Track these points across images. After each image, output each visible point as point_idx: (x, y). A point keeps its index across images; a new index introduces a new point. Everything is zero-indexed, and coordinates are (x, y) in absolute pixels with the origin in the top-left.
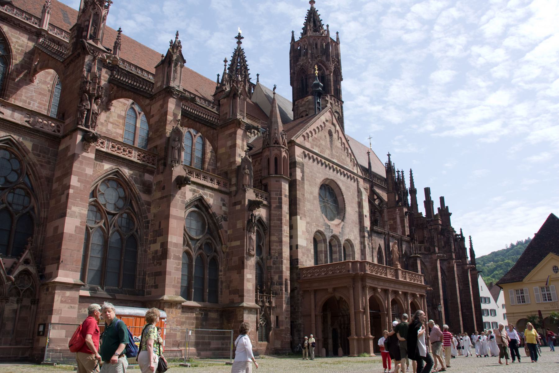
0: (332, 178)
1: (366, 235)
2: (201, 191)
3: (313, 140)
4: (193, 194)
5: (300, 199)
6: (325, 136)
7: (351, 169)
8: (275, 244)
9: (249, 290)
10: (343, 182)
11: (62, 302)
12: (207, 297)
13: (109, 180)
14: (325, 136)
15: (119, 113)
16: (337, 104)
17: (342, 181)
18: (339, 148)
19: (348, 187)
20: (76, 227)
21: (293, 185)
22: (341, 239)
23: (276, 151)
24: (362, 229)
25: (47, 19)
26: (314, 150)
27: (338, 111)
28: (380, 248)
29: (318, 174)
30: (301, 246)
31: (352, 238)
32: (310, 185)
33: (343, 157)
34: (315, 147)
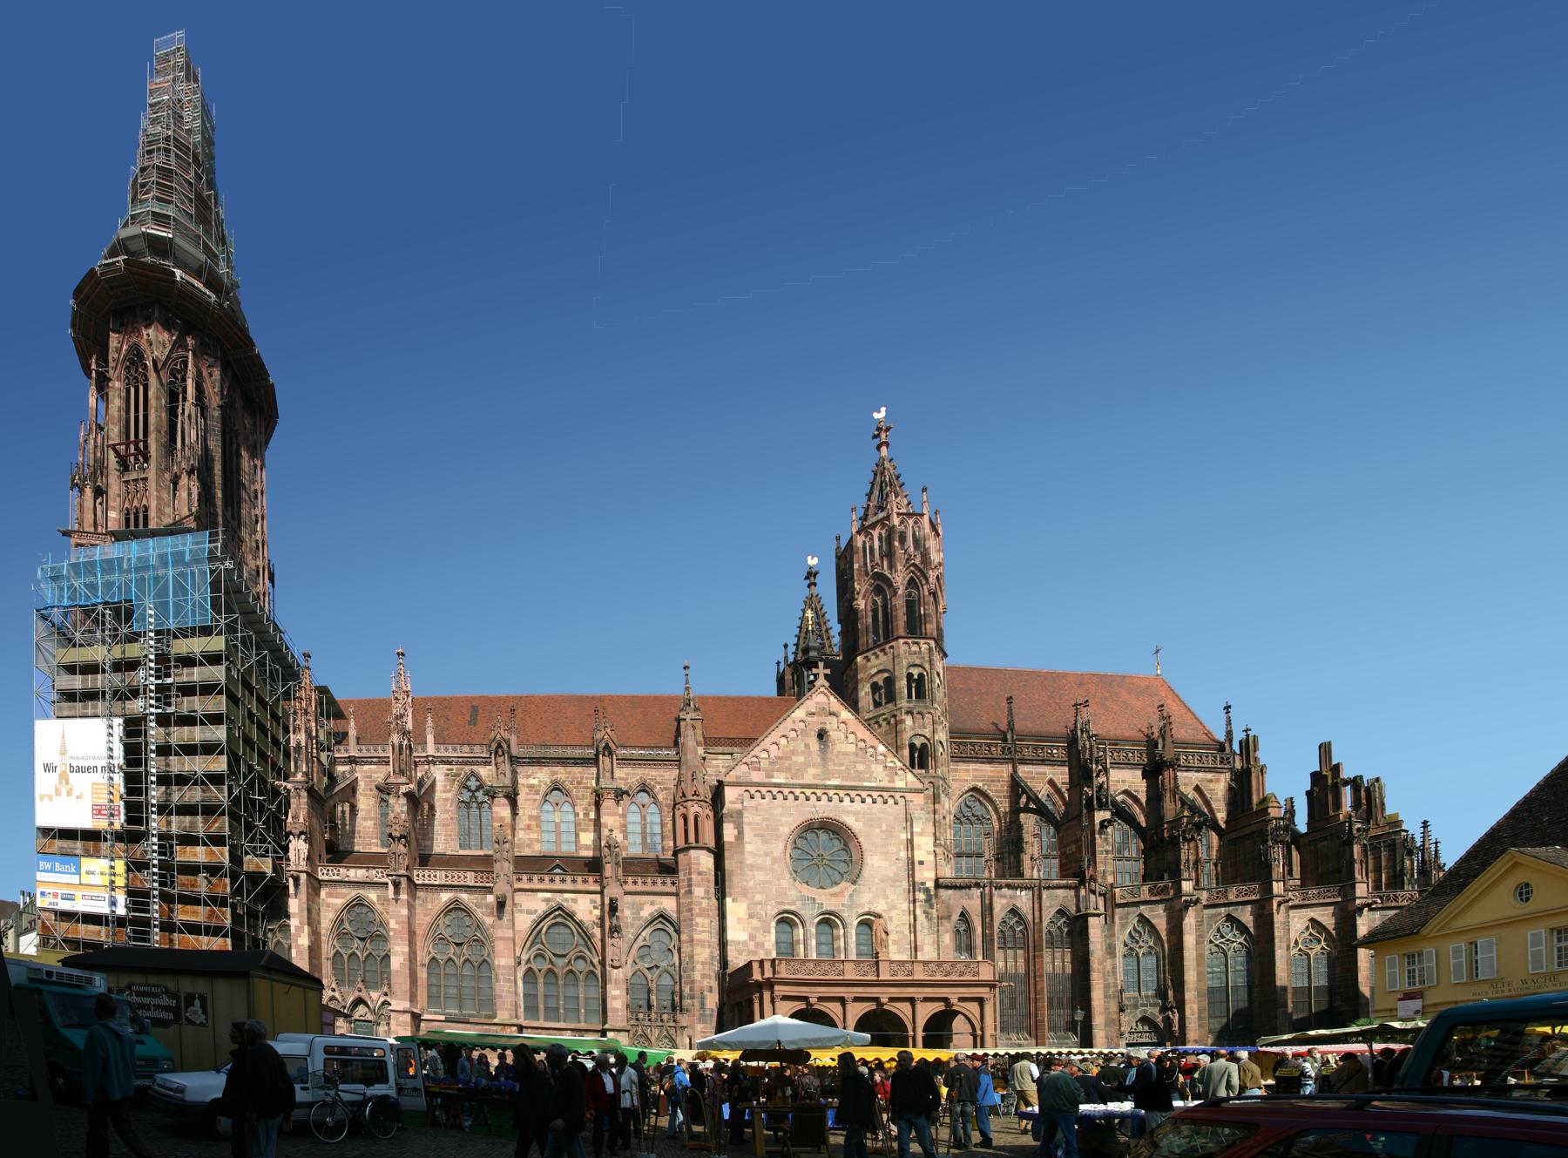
1: (921, 896)
6: (807, 746)
7: (885, 784)
10: (851, 814)
14: (807, 746)
16: (915, 648)
17: (855, 813)
18: (847, 754)
19: (869, 821)
21: (719, 853)
22: (845, 915)
23: (683, 810)
24: (914, 886)
27: (918, 662)
28: (964, 916)
31: (879, 907)
32: (764, 842)
33: (861, 767)
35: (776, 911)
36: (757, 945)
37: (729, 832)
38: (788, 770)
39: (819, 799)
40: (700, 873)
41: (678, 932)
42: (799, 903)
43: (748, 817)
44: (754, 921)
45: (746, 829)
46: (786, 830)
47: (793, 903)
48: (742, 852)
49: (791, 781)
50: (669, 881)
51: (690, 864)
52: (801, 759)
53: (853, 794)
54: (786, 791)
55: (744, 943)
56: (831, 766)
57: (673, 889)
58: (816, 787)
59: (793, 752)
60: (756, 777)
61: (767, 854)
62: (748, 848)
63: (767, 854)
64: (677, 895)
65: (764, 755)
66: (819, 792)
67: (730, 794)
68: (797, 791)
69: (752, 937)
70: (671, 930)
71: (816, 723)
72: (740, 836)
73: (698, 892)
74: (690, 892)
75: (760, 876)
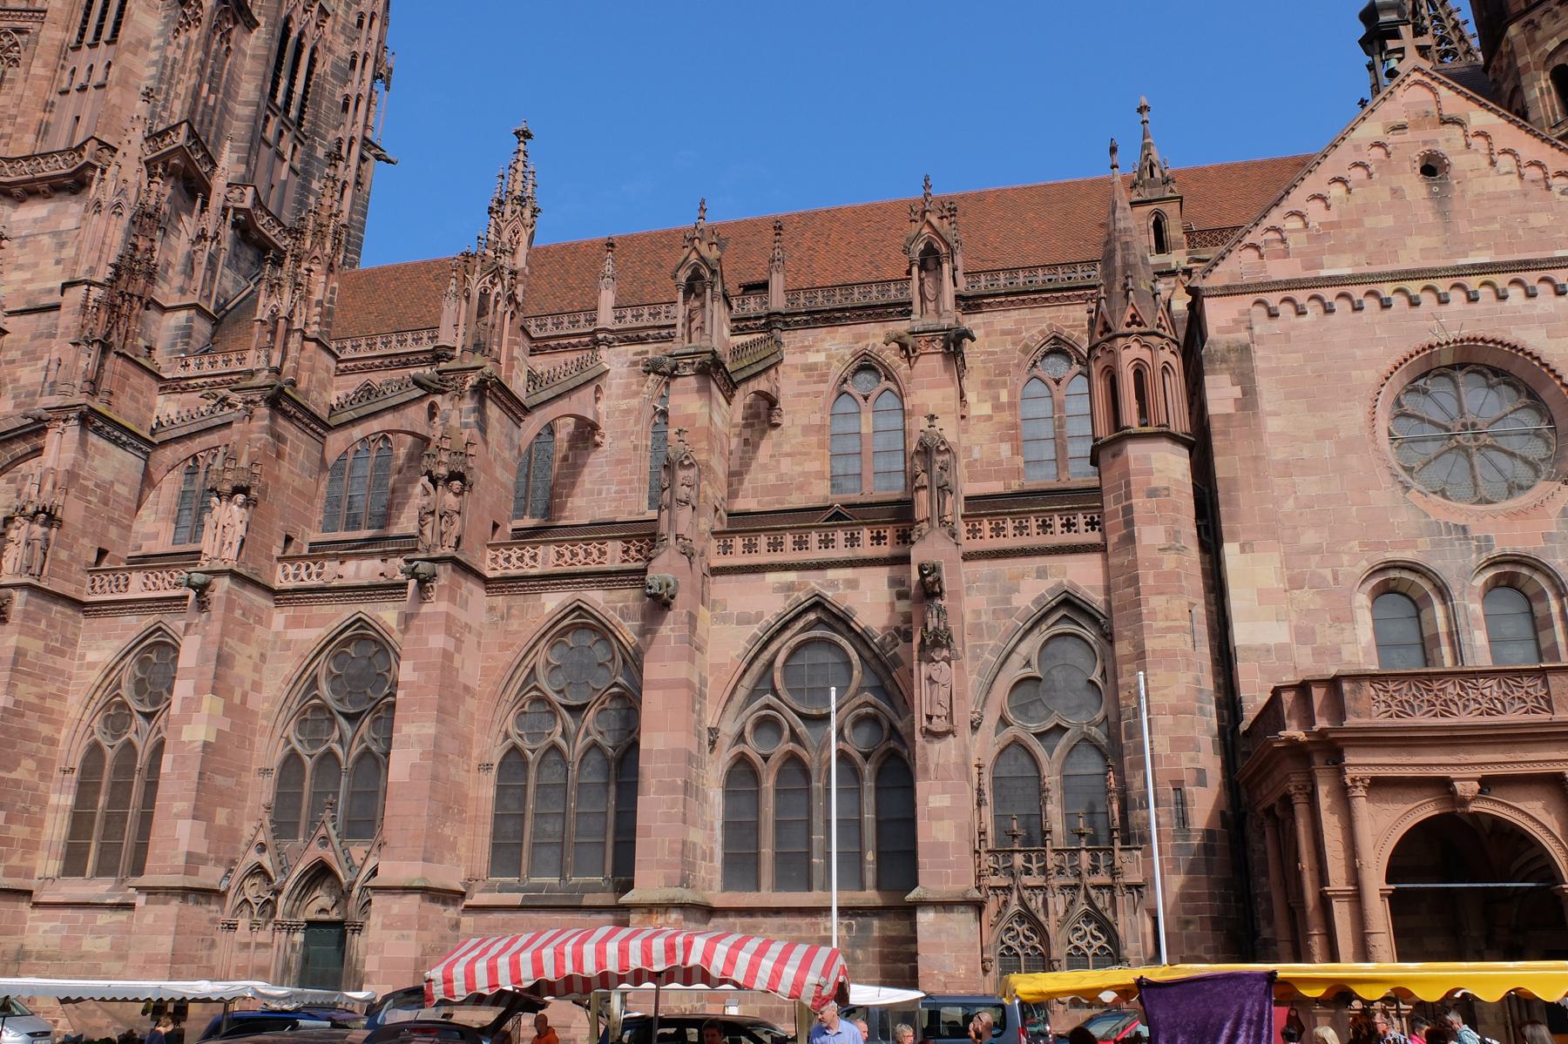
0: (1465, 333)
2: (815, 582)
3: (1315, 238)
4: (788, 597)
5: (1233, 482)
8: (1126, 667)
9: (945, 845)
11: (384, 926)
12: (870, 877)
13: (564, 632)
15: (806, 422)
17: (1546, 320)
20: (413, 766)
25: (607, 299)
26: (1324, 273)
29: (1358, 353)
30: (1249, 649)
33: (1540, 220)
34: (1326, 259)
35: (1364, 566)
36: (1319, 653)
37: (1220, 394)
38: (1359, 246)
39: (1443, 300)
40: (1152, 493)
41: (1108, 637)
42: (1424, 543)
43: (1262, 358)
44: (1305, 596)
45: (1263, 384)
46: (1371, 376)
47: (1410, 543)
48: (1256, 435)
49: (1366, 269)
50: (1081, 520)
51: (1126, 474)
52: (1387, 221)
53: (1531, 278)
54: (1357, 292)
55: (1281, 649)
56: (1463, 226)
57: (1094, 537)
58: (1434, 273)
59: (1365, 210)
60: (1279, 270)
61: (1322, 435)
62: (1272, 425)
63: (1322, 435)
64: (1100, 548)
65: (1295, 223)
66: (1442, 285)
67: (1217, 314)
68: (1386, 290)
69: (1303, 635)
70: (1090, 634)
71: (1412, 146)
72: (1248, 399)
73: (1150, 536)
74: (1129, 539)
75: (1309, 486)
